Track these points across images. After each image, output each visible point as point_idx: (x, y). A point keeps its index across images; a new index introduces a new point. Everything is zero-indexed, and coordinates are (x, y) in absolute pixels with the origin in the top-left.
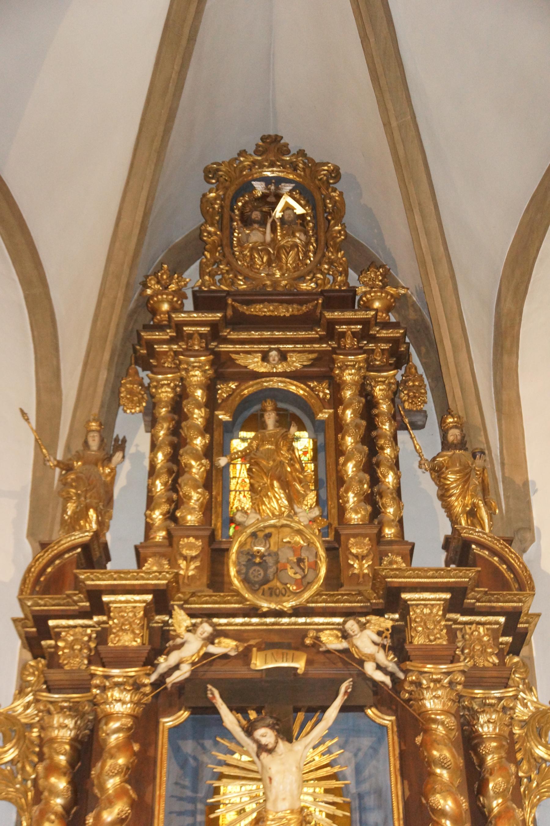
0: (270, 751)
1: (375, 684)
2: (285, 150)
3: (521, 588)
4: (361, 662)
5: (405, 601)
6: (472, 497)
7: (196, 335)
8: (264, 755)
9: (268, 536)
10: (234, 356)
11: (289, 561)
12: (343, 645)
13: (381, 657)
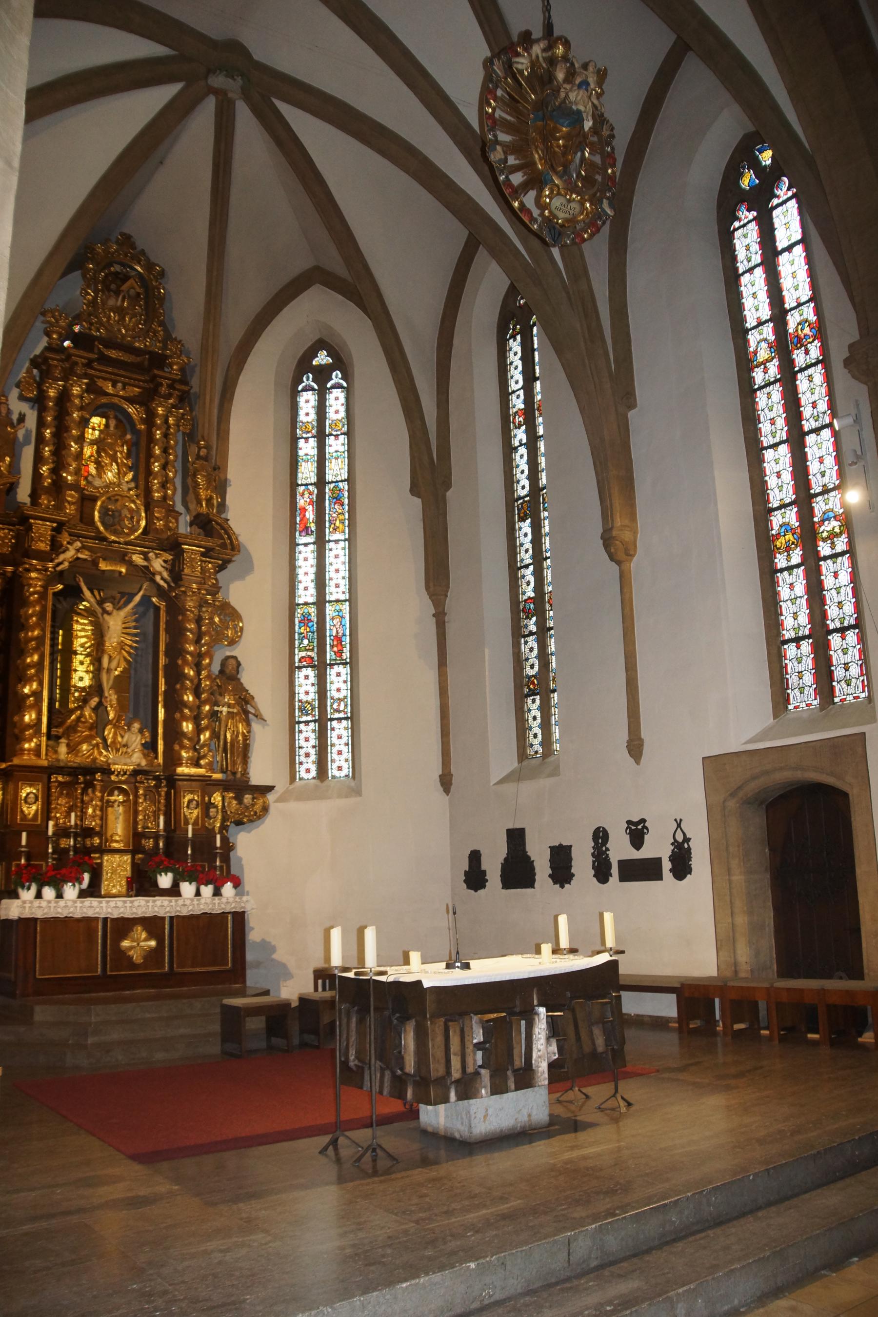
0: (109, 613)
1: (158, 585)
2: (133, 246)
3: (233, 549)
4: (154, 574)
5: (183, 549)
6: (212, 492)
7: (80, 365)
8: (105, 616)
9: (117, 500)
10: (96, 379)
11: (126, 517)
12: (145, 564)
13: (165, 574)
